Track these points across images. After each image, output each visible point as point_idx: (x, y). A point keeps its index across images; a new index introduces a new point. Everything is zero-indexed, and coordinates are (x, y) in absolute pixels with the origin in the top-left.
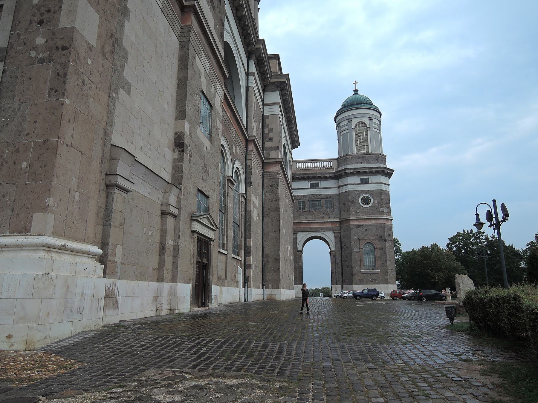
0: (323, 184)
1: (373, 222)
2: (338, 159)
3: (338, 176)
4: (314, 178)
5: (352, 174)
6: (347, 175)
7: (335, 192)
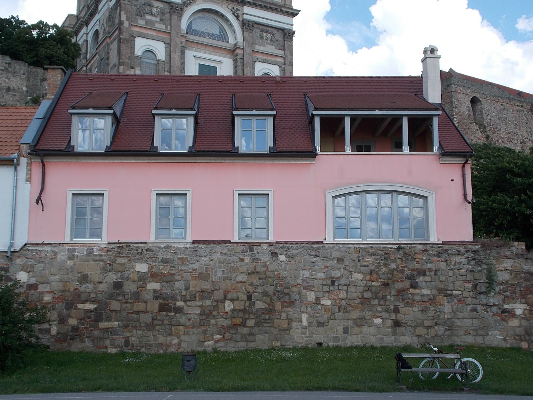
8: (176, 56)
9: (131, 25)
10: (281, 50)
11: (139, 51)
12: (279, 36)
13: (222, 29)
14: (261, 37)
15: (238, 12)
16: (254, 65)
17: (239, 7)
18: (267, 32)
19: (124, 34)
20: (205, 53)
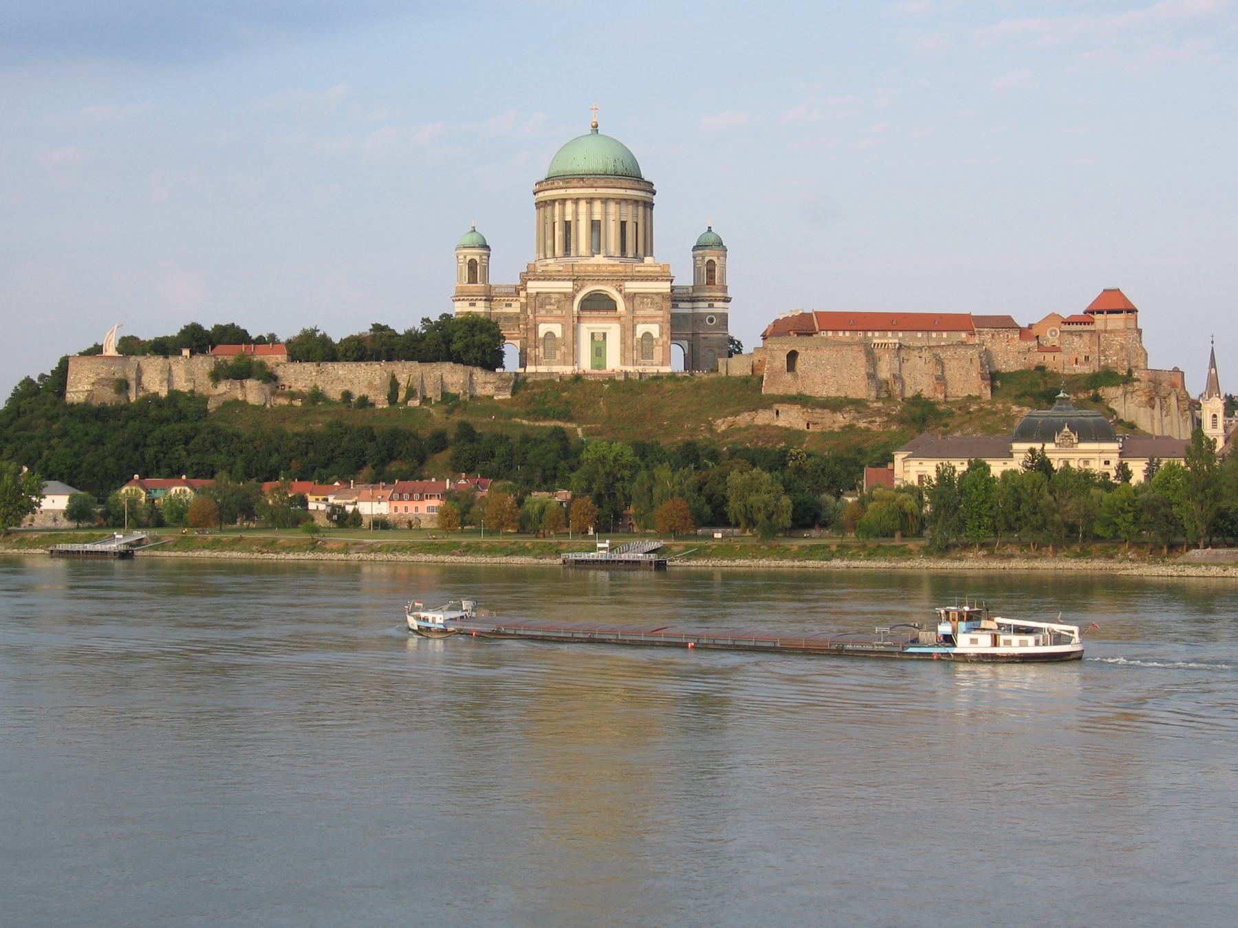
0: (681, 305)
1: (715, 336)
2: (693, 287)
3: (693, 300)
4: (675, 301)
5: (703, 301)
6: (699, 301)
7: (690, 311)
9: (535, 317)
11: (541, 334)
12: (658, 299)
14: (643, 303)
16: (634, 328)
17: (622, 283)
18: (647, 298)
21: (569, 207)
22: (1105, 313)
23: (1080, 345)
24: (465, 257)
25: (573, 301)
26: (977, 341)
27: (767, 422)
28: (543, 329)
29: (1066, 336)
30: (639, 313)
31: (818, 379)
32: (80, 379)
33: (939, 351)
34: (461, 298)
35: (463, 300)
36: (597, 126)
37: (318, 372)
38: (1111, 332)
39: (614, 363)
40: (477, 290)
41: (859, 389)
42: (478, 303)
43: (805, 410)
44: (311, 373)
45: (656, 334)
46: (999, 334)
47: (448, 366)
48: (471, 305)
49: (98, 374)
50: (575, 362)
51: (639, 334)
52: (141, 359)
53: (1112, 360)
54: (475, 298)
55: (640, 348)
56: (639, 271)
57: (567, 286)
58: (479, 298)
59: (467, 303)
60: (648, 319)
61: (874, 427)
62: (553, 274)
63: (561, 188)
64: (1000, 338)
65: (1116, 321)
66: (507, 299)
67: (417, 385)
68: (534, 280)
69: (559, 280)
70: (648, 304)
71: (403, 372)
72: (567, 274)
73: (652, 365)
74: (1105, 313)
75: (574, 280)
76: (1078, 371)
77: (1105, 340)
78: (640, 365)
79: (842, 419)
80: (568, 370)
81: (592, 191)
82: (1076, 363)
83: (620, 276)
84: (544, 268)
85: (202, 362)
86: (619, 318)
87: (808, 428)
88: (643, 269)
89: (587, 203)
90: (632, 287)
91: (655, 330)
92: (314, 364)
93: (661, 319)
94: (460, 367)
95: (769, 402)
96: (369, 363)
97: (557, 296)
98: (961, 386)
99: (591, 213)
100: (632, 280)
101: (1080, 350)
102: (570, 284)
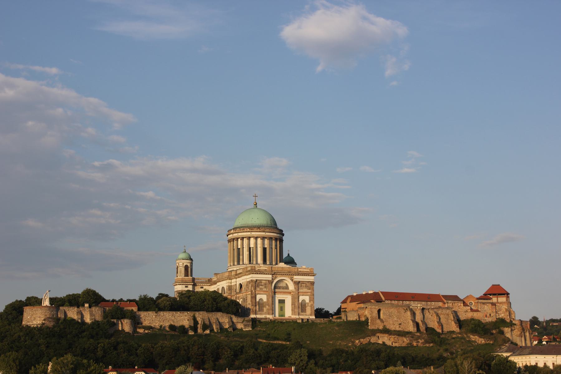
8: (270, 299)
10: (309, 289)
11: (258, 300)
12: (308, 284)
13: (286, 284)
14: (301, 286)
15: (292, 278)
16: (298, 297)
17: (293, 276)
18: (304, 283)
19: (253, 295)
20: (281, 295)
21: (252, 241)
22: (497, 295)
23: (487, 308)
24: (183, 264)
25: (272, 284)
26: (446, 306)
27: (375, 342)
28: (258, 297)
29: (483, 305)
30: (300, 290)
31: (391, 322)
32: (35, 318)
33: (436, 310)
34: (182, 283)
35: (183, 284)
36: (256, 204)
37: (156, 316)
38: (501, 303)
39: (289, 313)
40: (188, 280)
41: (411, 328)
42: (189, 286)
43: (391, 336)
44: (152, 316)
45: (307, 301)
46: (455, 303)
47: (219, 315)
48: (186, 287)
49: (46, 315)
50: (273, 313)
51: (300, 301)
52: (65, 308)
53: (502, 315)
54: (188, 284)
55: (301, 307)
56: (300, 271)
57: (269, 277)
58: (190, 284)
59: (184, 286)
60: (304, 294)
61: (420, 344)
62: (263, 271)
63: (248, 232)
64: (455, 305)
65: (502, 299)
66: (202, 284)
67: (207, 322)
68: (255, 273)
69: (266, 274)
70: (304, 286)
71: (199, 317)
72: (269, 271)
73: (306, 315)
74: (497, 295)
75: (273, 274)
76: (487, 321)
77: (498, 307)
78: (301, 315)
79: (406, 341)
80: (270, 317)
81: (263, 233)
82: (486, 317)
83: (293, 273)
84: (259, 268)
85: (98, 311)
86: (290, 293)
87: (392, 344)
88: (302, 270)
89: (261, 239)
90: (297, 278)
91: (307, 299)
92: (154, 312)
93: (310, 294)
94: (225, 315)
95: (374, 332)
96: (182, 312)
97: (264, 282)
98: (446, 327)
99: (263, 244)
100: (298, 275)
101: (487, 311)
102: (271, 276)
